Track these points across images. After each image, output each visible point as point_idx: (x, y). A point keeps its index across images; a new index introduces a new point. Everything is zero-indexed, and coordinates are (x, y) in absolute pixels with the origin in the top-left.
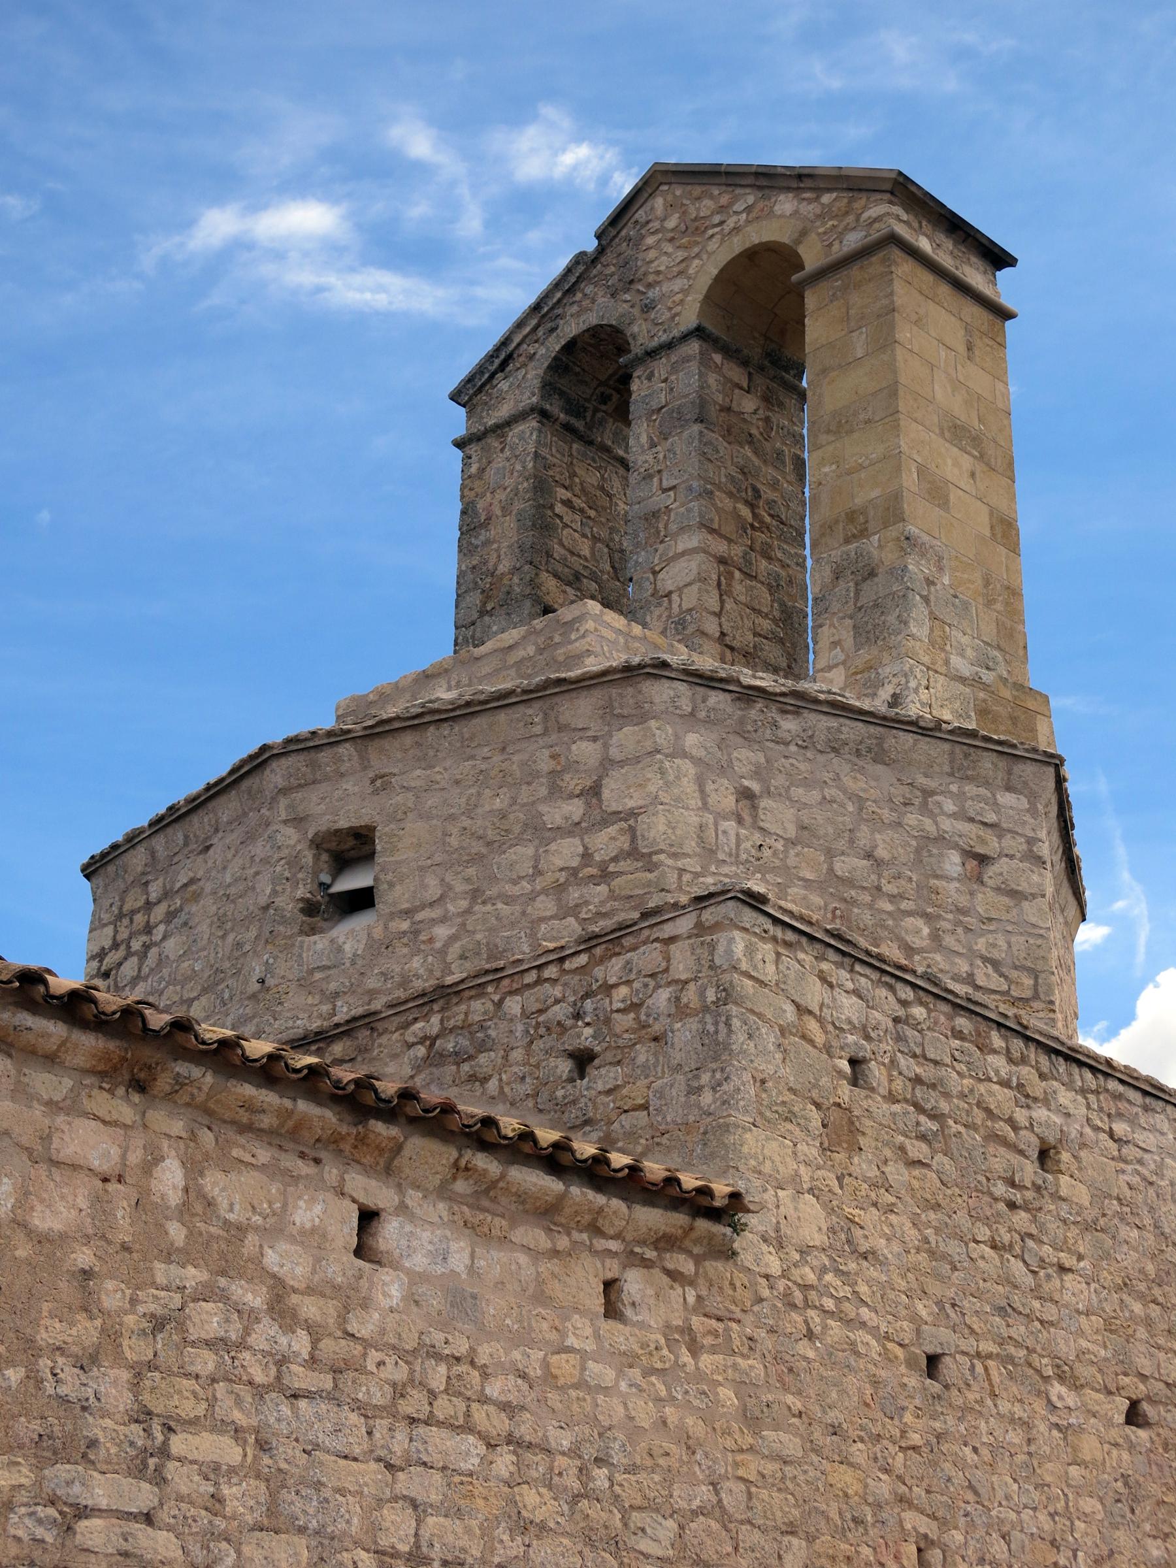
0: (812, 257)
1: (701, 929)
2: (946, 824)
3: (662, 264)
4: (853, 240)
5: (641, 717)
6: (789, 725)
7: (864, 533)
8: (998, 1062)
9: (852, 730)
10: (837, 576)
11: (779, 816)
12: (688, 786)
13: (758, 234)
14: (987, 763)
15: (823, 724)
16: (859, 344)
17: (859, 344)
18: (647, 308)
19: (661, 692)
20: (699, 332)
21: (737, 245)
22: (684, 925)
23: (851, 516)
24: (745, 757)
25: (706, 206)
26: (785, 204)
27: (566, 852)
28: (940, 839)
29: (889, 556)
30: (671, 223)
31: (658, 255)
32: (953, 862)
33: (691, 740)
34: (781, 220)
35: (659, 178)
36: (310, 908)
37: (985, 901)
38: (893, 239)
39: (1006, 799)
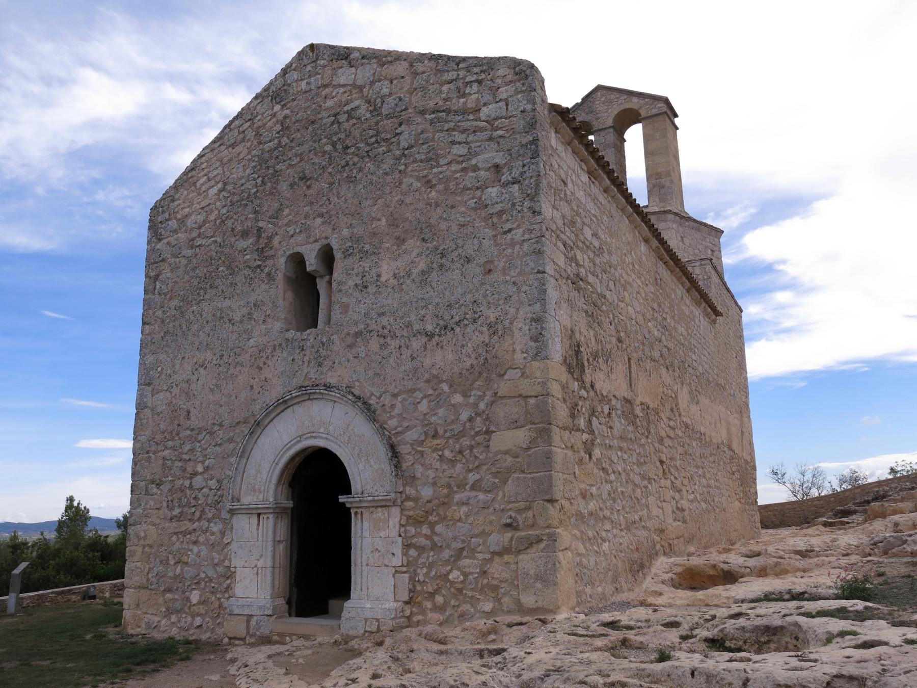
0: (643, 113)
1: (701, 265)
3: (601, 109)
4: (654, 111)
5: (666, 221)
7: (660, 178)
10: (654, 187)
11: (686, 241)
13: (627, 106)
16: (658, 135)
17: (658, 135)
18: (597, 119)
19: (670, 216)
20: (613, 127)
21: (622, 108)
22: (698, 264)
23: (657, 174)
24: (681, 230)
25: (612, 97)
26: (635, 100)
29: (668, 184)
30: (603, 99)
31: (599, 106)
34: (634, 103)
35: (599, 88)
38: (666, 113)
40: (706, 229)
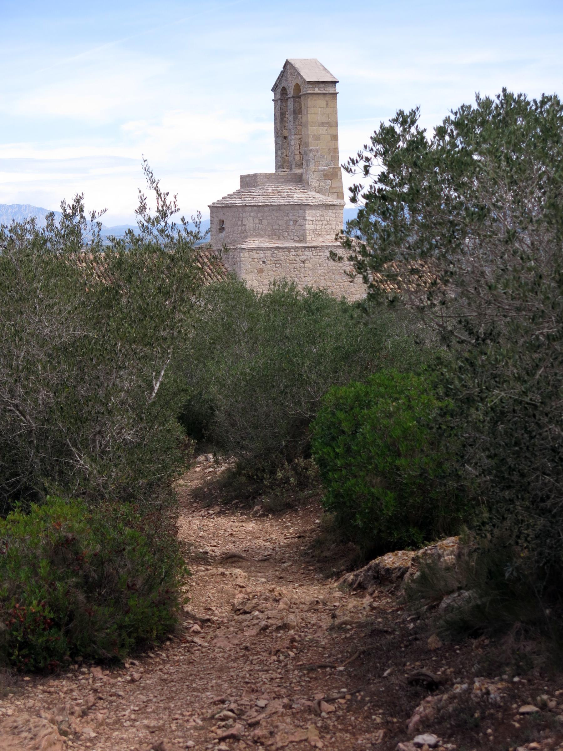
2: (290, 218)
6: (266, 209)
8: (293, 253)
9: (275, 208)
11: (265, 222)
12: (251, 221)
14: (297, 208)
15: (271, 207)
19: (247, 209)
20: (293, 97)
24: (260, 215)
27: (240, 228)
28: (290, 220)
32: (292, 223)
33: (252, 214)
36: (220, 229)
37: (297, 227)
39: (300, 211)
40: (289, 208)
